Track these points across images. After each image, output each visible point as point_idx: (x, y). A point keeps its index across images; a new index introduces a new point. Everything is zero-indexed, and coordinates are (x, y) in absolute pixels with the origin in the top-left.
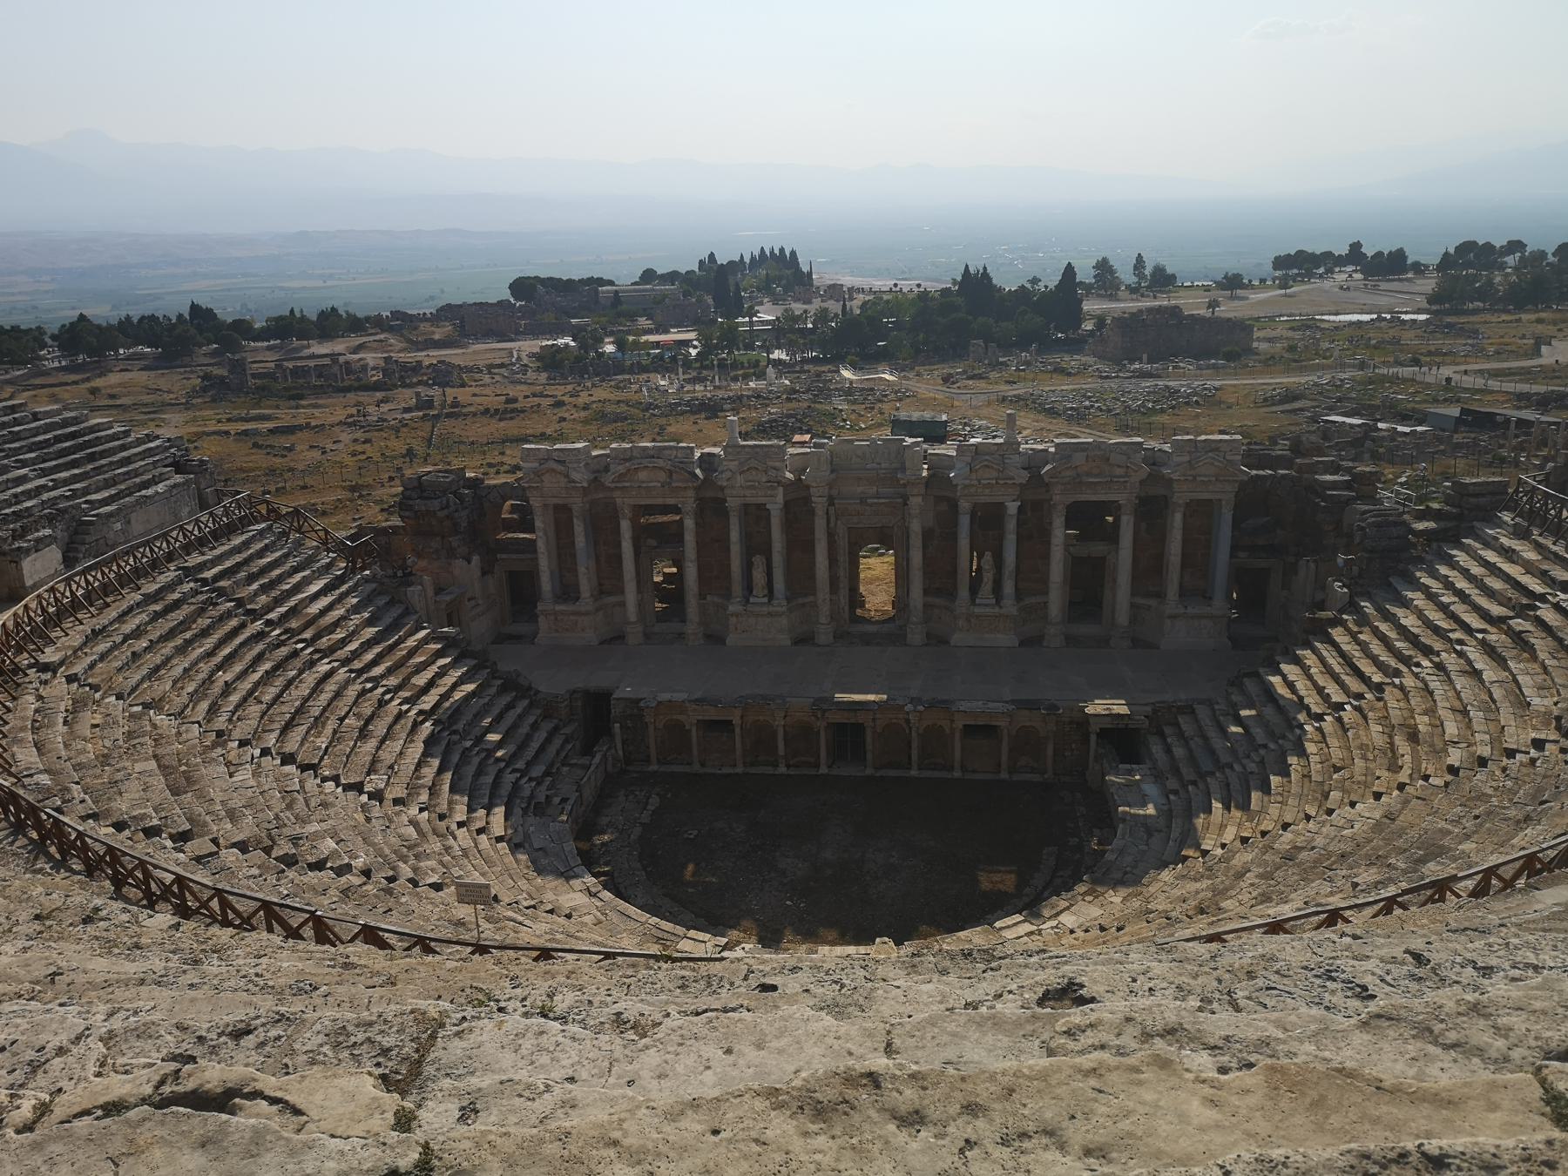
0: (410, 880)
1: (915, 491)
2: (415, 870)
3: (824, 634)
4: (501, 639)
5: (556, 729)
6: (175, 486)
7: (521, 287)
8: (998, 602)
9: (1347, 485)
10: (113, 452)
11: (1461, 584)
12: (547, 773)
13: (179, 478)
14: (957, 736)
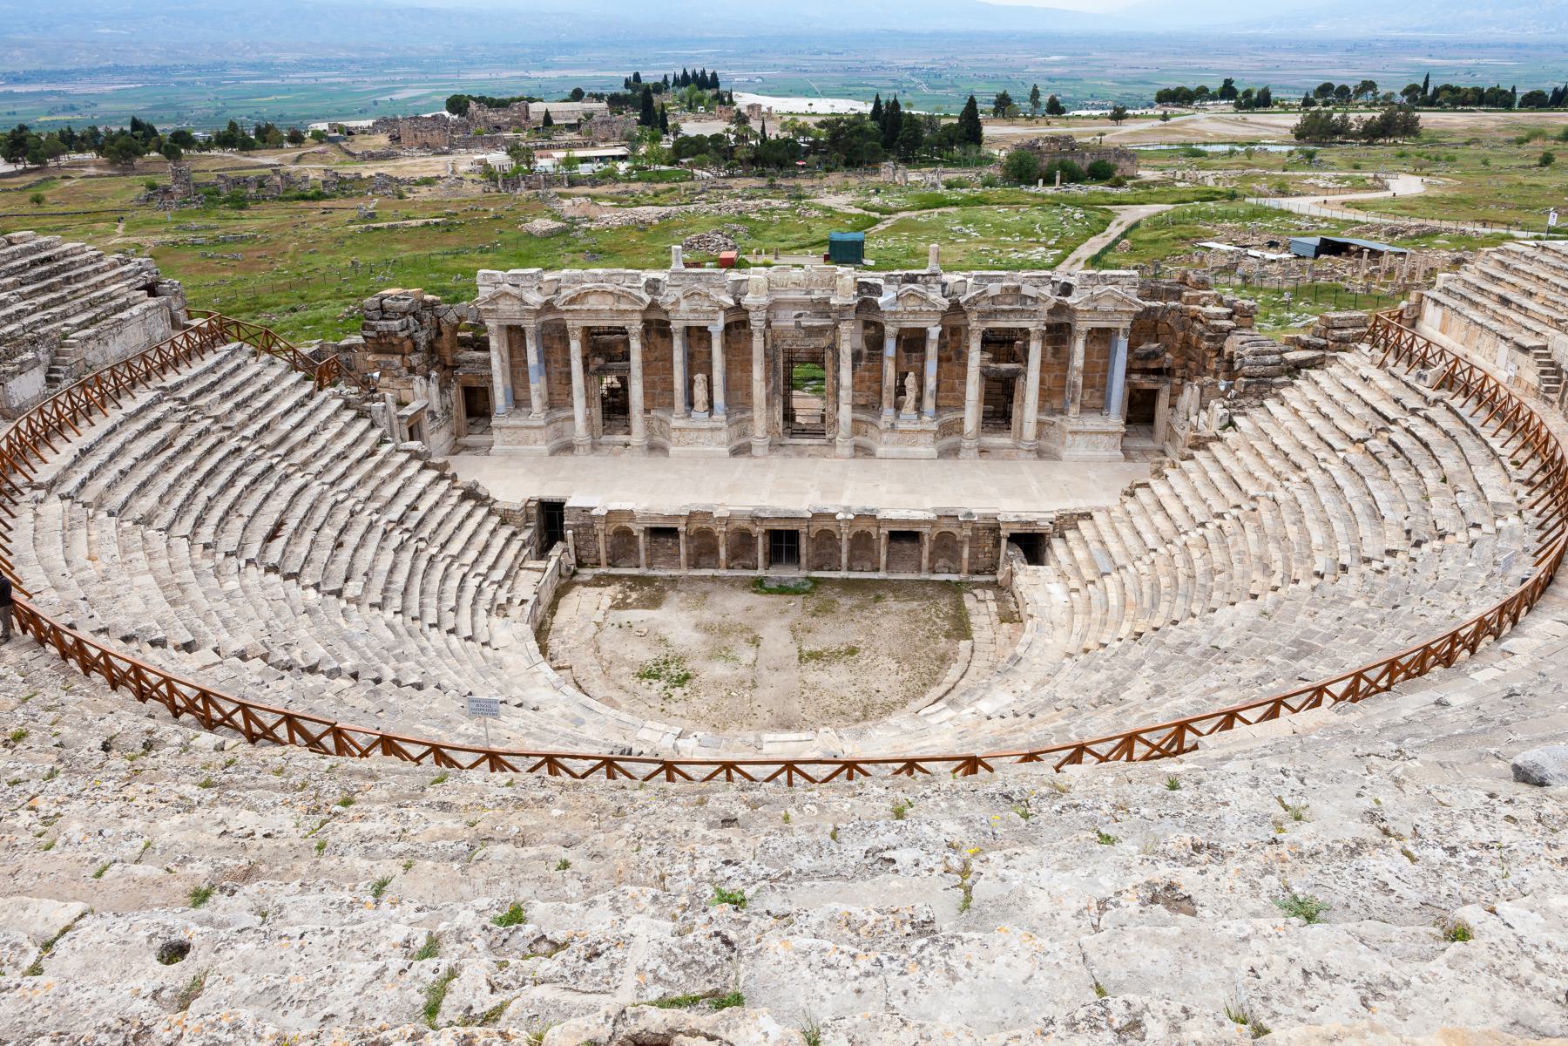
0: (394, 681)
2: (397, 670)
4: (457, 449)
5: (514, 534)
6: (148, 309)
7: (457, 104)
9: (1230, 317)
10: (86, 276)
11: (1326, 408)
12: (507, 576)
13: (152, 302)
14: (883, 541)
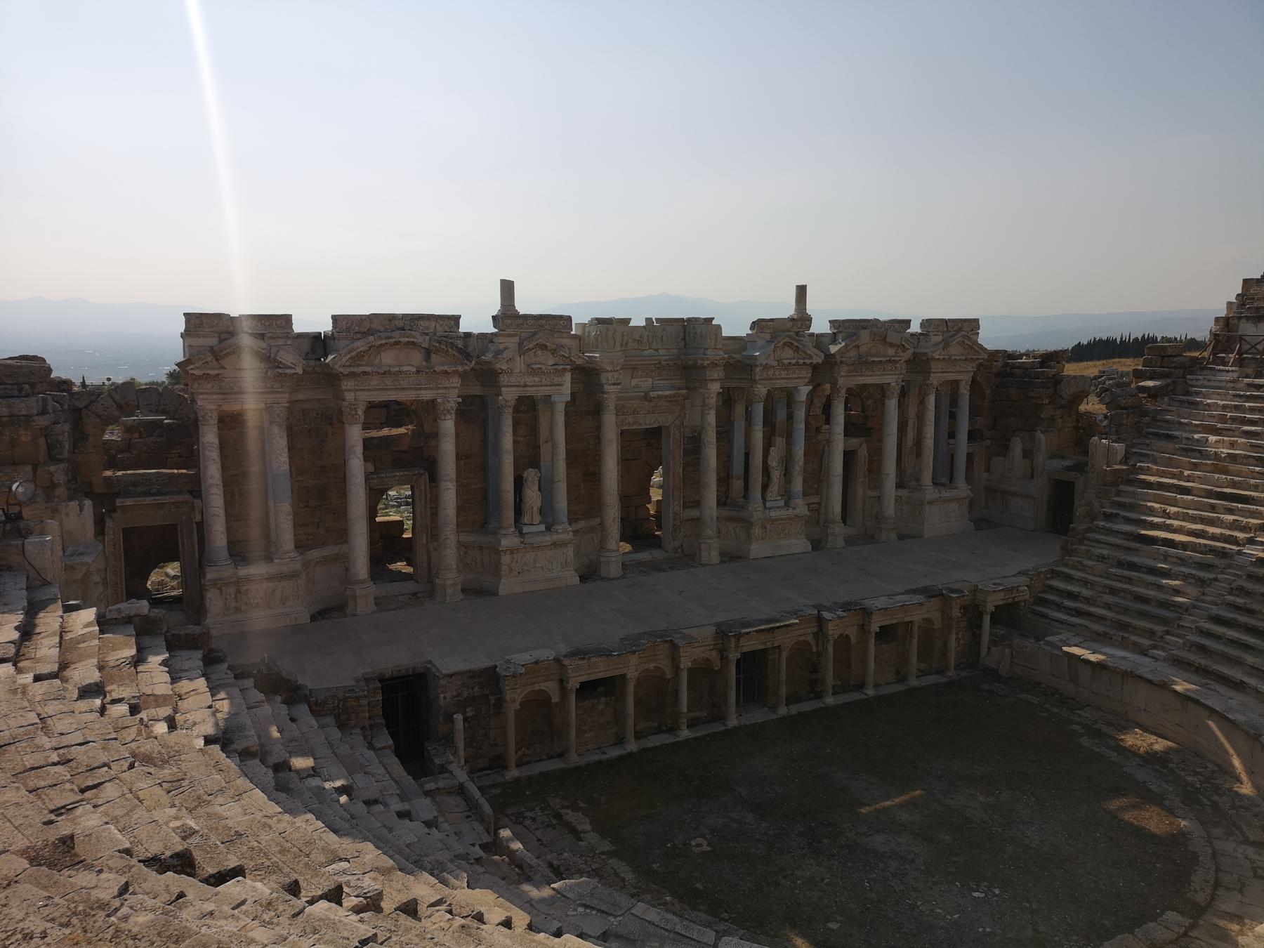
1: (715, 376)
8: (787, 504)
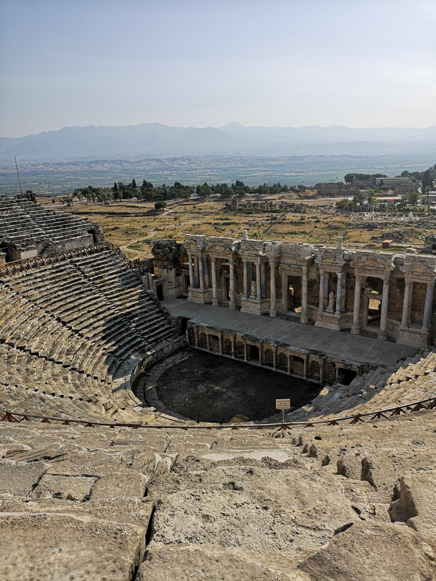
1: (304, 264)
3: (272, 314)
5: (170, 328)
7: (348, 178)
